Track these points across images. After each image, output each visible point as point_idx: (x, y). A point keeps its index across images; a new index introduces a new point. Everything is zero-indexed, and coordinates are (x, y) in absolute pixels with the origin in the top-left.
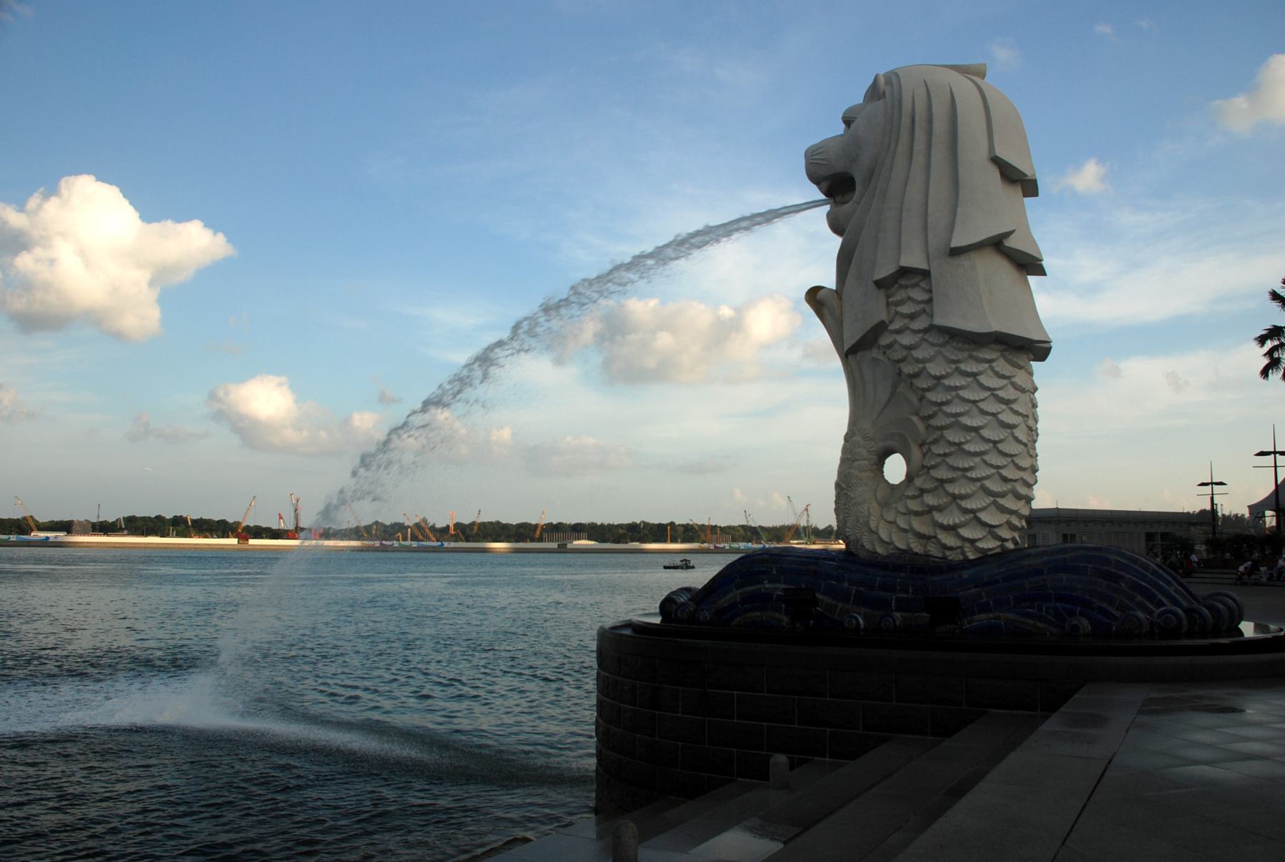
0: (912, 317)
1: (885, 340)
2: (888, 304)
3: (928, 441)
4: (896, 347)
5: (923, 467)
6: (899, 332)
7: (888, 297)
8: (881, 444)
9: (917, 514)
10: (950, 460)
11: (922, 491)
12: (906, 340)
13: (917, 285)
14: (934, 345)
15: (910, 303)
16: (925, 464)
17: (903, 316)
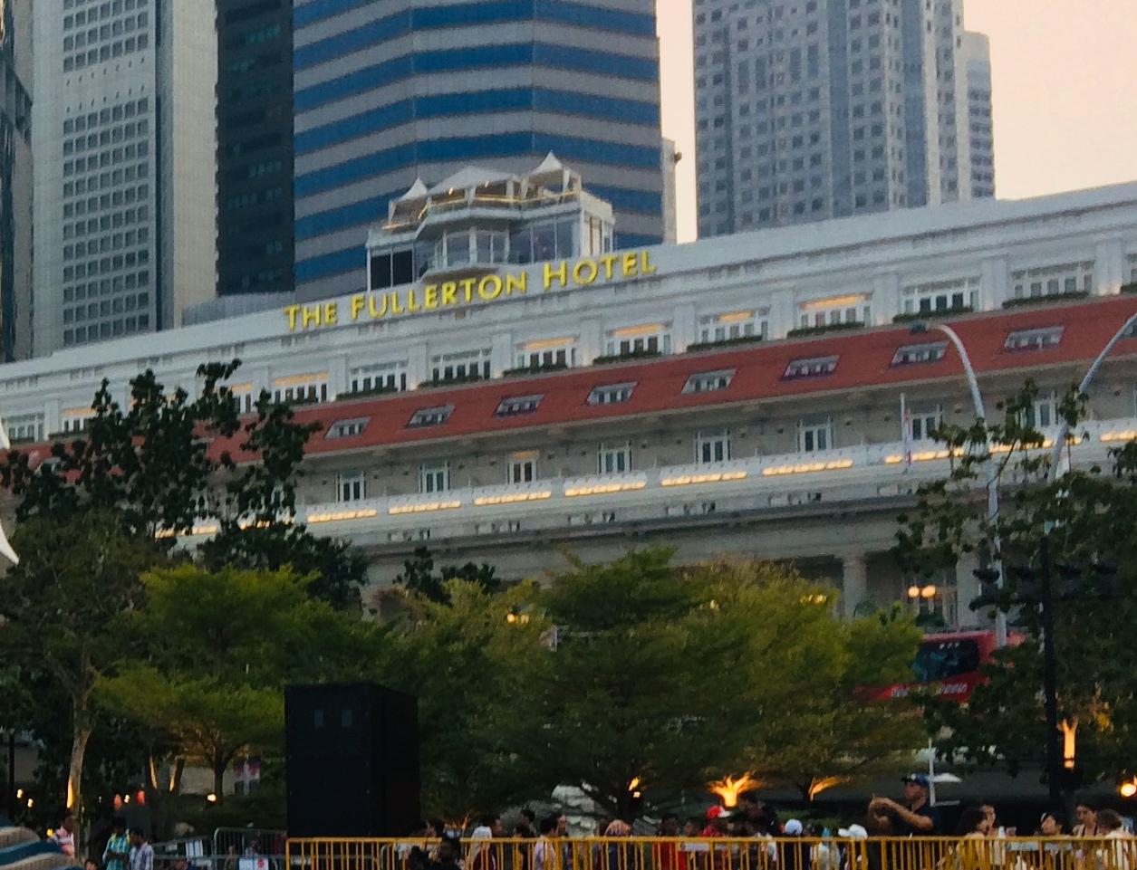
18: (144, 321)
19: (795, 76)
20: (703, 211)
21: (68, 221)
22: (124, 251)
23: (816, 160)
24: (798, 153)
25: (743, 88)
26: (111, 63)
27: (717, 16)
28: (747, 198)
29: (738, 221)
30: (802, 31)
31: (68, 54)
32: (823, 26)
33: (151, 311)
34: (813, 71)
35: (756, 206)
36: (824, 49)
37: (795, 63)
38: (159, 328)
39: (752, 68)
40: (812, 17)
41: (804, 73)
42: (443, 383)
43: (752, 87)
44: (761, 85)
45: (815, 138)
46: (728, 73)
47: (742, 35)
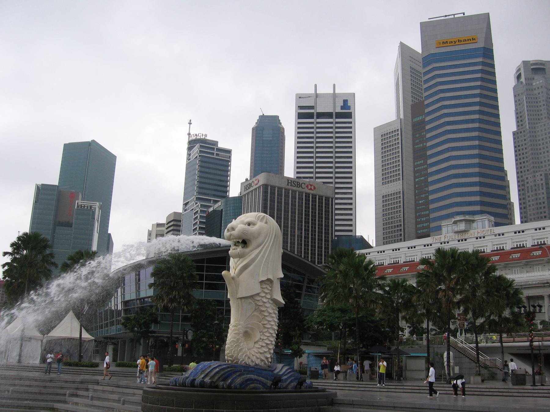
0: (266, 293)
1: (259, 298)
2: (261, 288)
3: (264, 331)
4: (261, 301)
5: (261, 339)
6: (263, 297)
7: (261, 285)
8: (245, 329)
9: (261, 353)
10: (269, 338)
11: (262, 346)
12: (265, 300)
13: (269, 284)
14: (270, 303)
15: (266, 289)
16: (262, 338)
17: (264, 292)
18: (401, 240)
19: (539, 190)
20: (521, 218)
21: (384, 218)
22: (396, 224)
23: (544, 207)
24: (541, 206)
25: (528, 192)
26: (392, 184)
27: (522, 177)
28: (530, 215)
29: (529, 220)
30: (540, 180)
31: (383, 182)
32: (544, 179)
33: (402, 238)
34: (542, 189)
35: (532, 217)
36: (544, 184)
37: (539, 187)
38: (404, 241)
39: (530, 187)
40: (541, 177)
41: (541, 189)
42: (395, 263)
43: (530, 192)
44: (532, 191)
45: (544, 203)
46: (525, 188)
47: (527, 181)
